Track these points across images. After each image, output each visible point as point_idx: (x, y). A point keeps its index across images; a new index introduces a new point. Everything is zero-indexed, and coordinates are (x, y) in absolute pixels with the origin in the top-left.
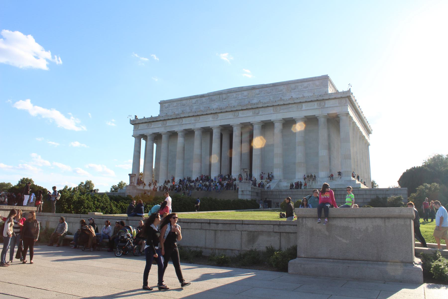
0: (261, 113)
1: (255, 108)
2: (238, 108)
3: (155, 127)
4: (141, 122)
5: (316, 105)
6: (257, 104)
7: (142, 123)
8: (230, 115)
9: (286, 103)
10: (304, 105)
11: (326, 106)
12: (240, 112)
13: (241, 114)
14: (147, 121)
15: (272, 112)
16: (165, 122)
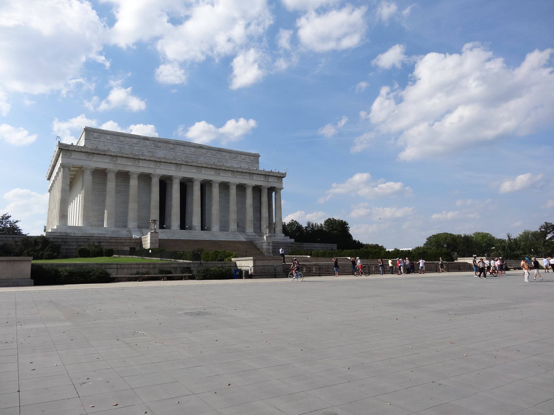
0: (221, 174)
1: (218, 169)
2: (203, 165)
3: (99, 160)
4: (79, 150)
5: (262, 178)
6: (221, 166)
7: (81, 152)
8: (194, 170)
9: (243, 171)
10: (254, 175)
11: (269, 180)
12: (203, 169)
13: (203, 171)
14: (89, 151)
15: (230, 175)
16: (114, 159)
